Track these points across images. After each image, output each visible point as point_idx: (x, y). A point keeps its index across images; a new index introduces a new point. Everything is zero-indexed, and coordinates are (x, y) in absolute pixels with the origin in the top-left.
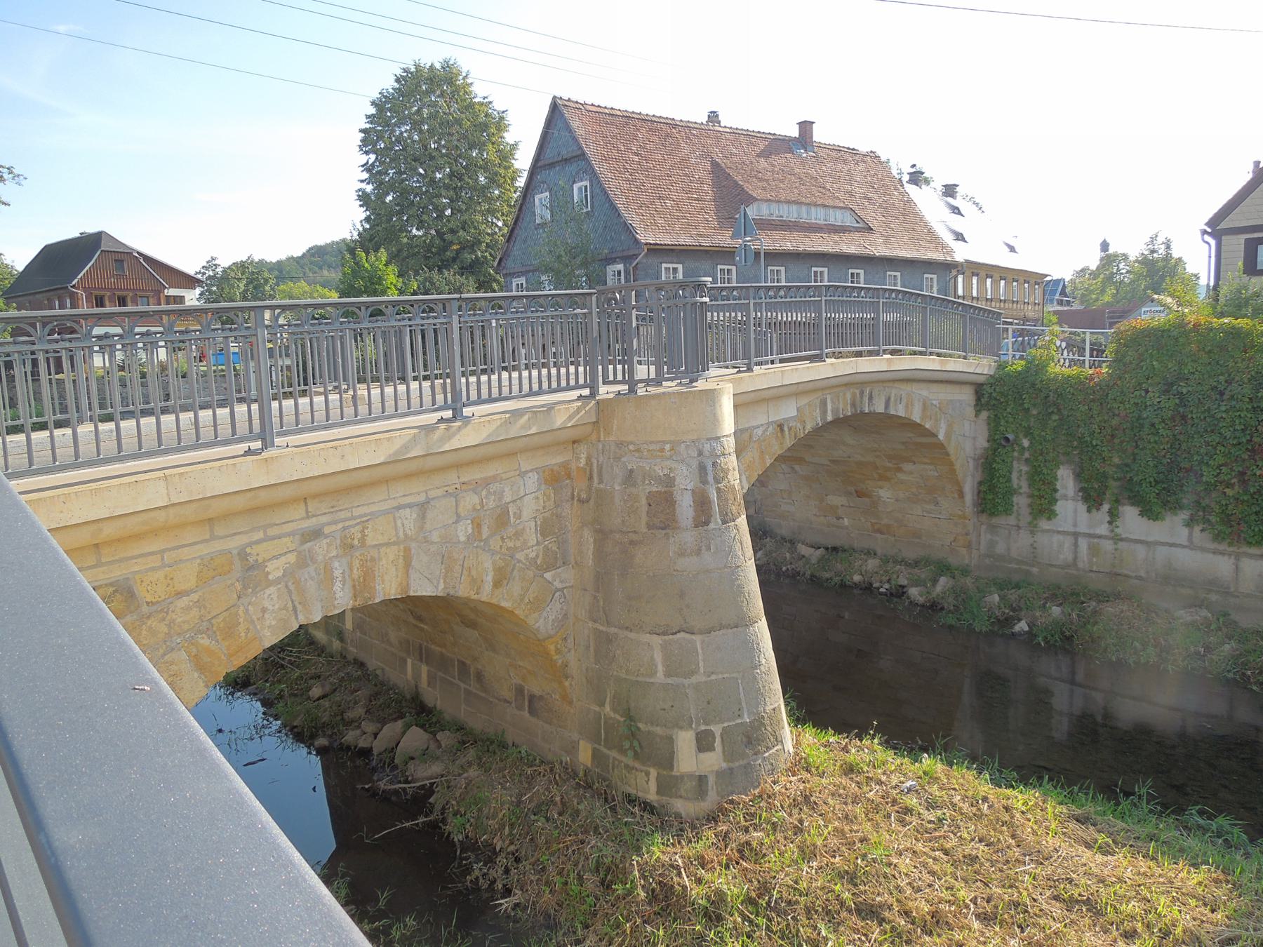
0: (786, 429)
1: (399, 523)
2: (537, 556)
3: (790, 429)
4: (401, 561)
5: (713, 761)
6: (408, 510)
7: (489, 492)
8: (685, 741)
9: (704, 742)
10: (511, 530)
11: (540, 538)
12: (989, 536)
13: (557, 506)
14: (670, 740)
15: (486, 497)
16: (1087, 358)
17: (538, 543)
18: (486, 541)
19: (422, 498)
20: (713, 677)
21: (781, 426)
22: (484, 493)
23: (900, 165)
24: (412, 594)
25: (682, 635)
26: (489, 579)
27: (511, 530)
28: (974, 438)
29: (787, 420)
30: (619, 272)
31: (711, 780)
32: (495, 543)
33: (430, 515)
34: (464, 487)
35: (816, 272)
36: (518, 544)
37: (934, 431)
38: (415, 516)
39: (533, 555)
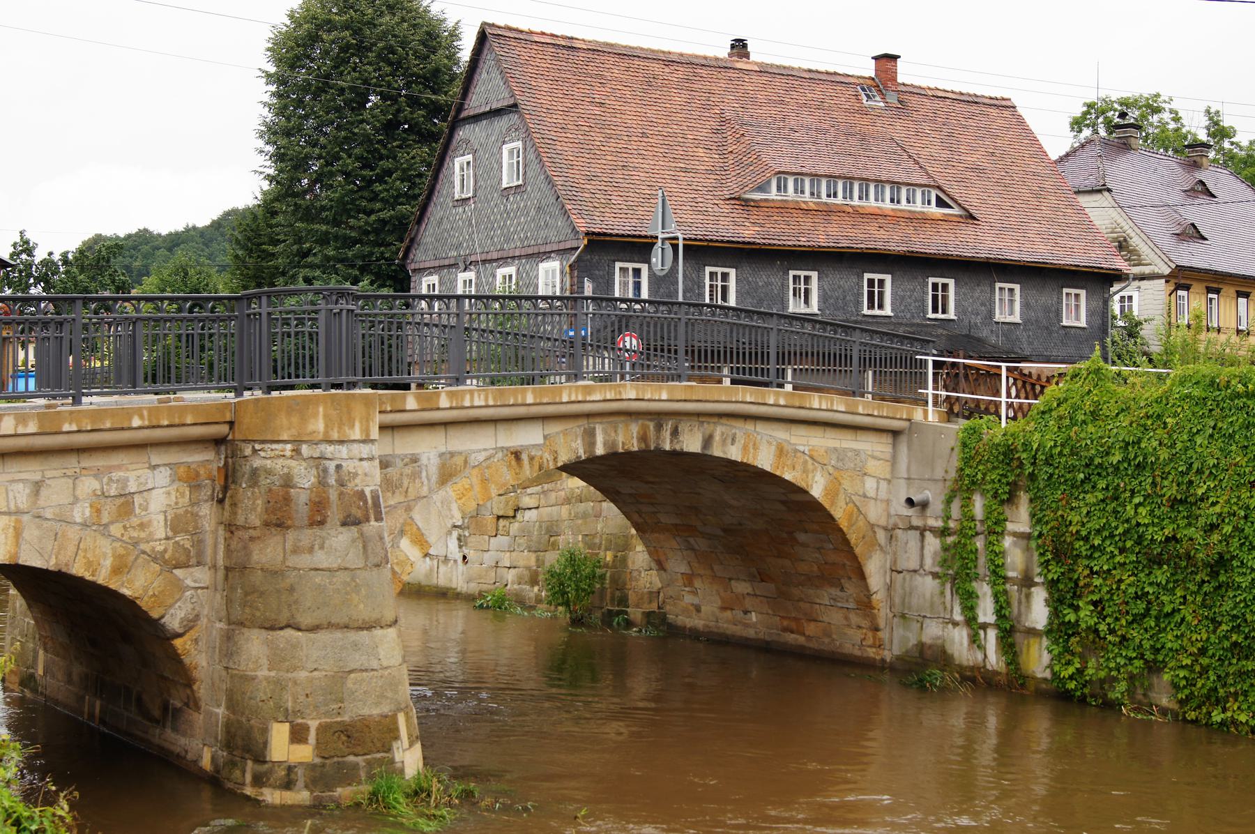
0: (524, 457)
1: (11, 495)
2: (165, 551)
3: (532, 459)
4: (11, 530)
5: (304, 753)
6: (21, 485)
7: (110, 479)
8: (279, 735)
9: (298, 735)
10: (135, 521)
11: (170, 534)
12: (901, 631)
13: (192, 504)
14: (265, 731)
15: (108, 484)
16: (1003, 399)
17: (167, 538)
18: (106, 526)
19: (38, 477)
20: (315, 673)
21: (517, 455)
22: (105, 480)
23: (12, 249)
24: (20, 562)
25: (289, 632)
26: (108, 563)
27: (135, 521)
28: (888, 502)
29: (527, 447)
30: (510, 276)
31: (300, 772)
32: (116, 529)
33: (44, 492)
34: (84, 472)
35: (795, 277)
36: (143, 535)
37: (803, 484)
38: (27, 491)
39: (160, 548)
